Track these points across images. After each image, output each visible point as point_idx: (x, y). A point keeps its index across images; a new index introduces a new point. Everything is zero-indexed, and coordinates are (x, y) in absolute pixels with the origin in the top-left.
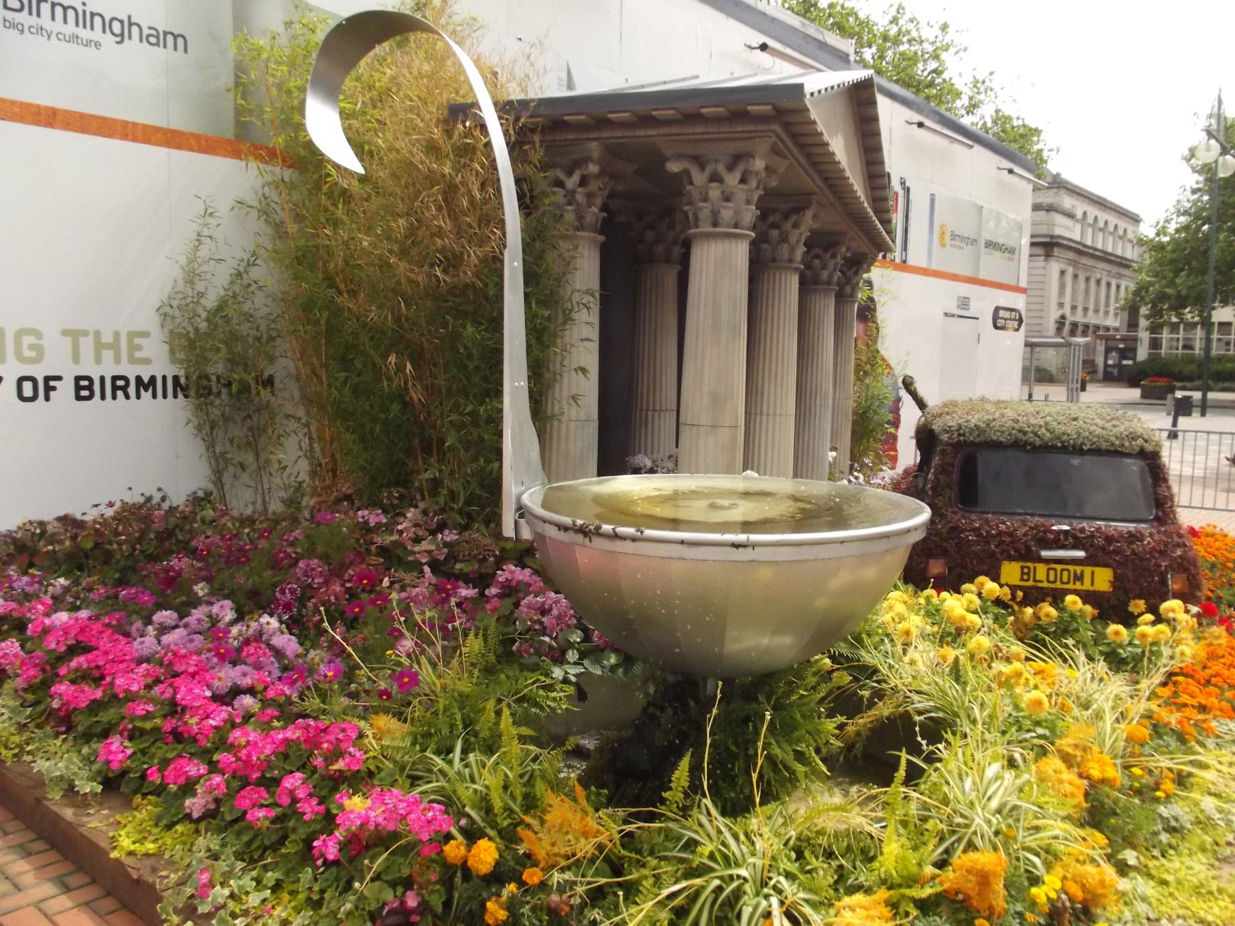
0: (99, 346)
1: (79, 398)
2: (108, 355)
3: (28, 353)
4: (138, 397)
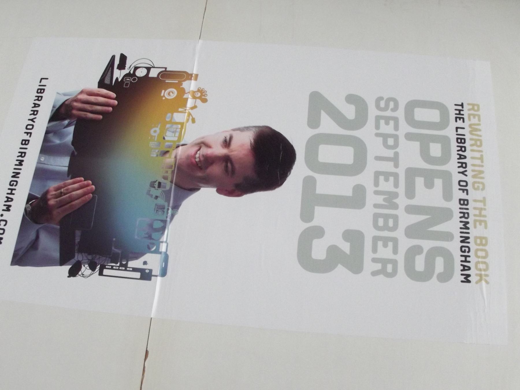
0: (481, 209)
1: (460, 200)
2: (477, 212)
3: (476, 185)
4: (461, 222)
